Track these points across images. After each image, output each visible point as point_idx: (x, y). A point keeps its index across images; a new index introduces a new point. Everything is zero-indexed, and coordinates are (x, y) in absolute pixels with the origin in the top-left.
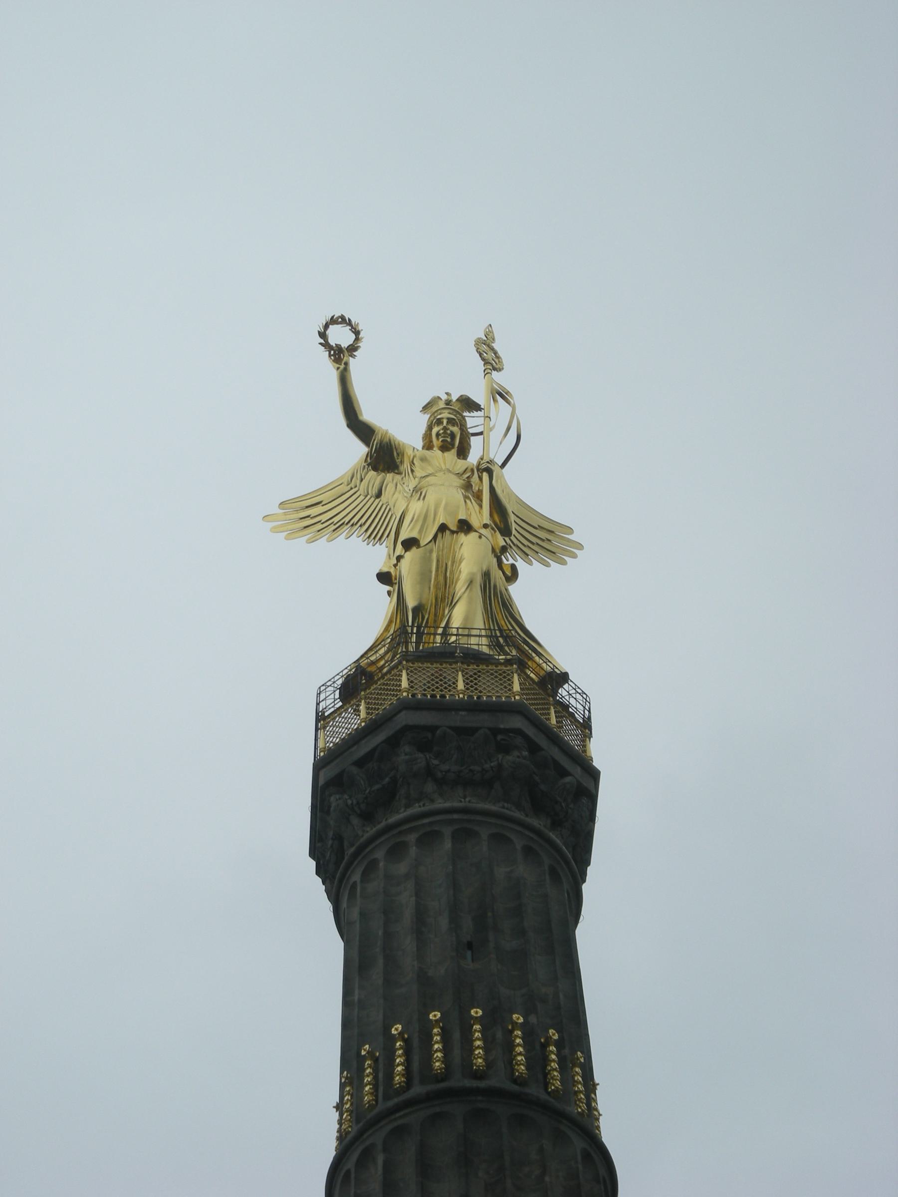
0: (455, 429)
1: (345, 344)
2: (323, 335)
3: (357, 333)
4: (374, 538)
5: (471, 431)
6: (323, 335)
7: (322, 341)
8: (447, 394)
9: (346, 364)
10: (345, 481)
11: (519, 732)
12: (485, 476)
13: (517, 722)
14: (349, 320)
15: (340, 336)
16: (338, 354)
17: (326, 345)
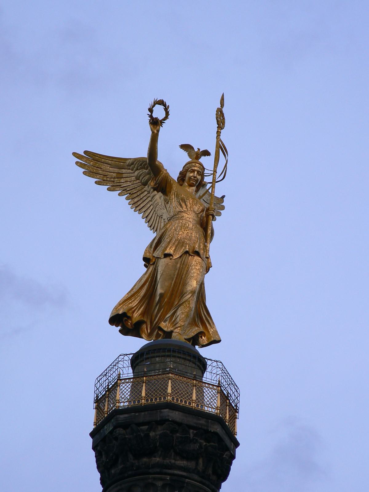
0: (199, 177)
1: (161, 118)
2: (151, 110)
3: (167, 114)
4: (136, 207)
5: (205, 175)
6: (151, 110)
7: (150, 114)
8: (199, 149)
9: (158, 131)
10: (128, 162)
11: (216, 434)
12: (211, 217)
13: (217, 428)
14: (166, 104)
15: (159, 112)
16: (155, 123)
17: (151, 116)
